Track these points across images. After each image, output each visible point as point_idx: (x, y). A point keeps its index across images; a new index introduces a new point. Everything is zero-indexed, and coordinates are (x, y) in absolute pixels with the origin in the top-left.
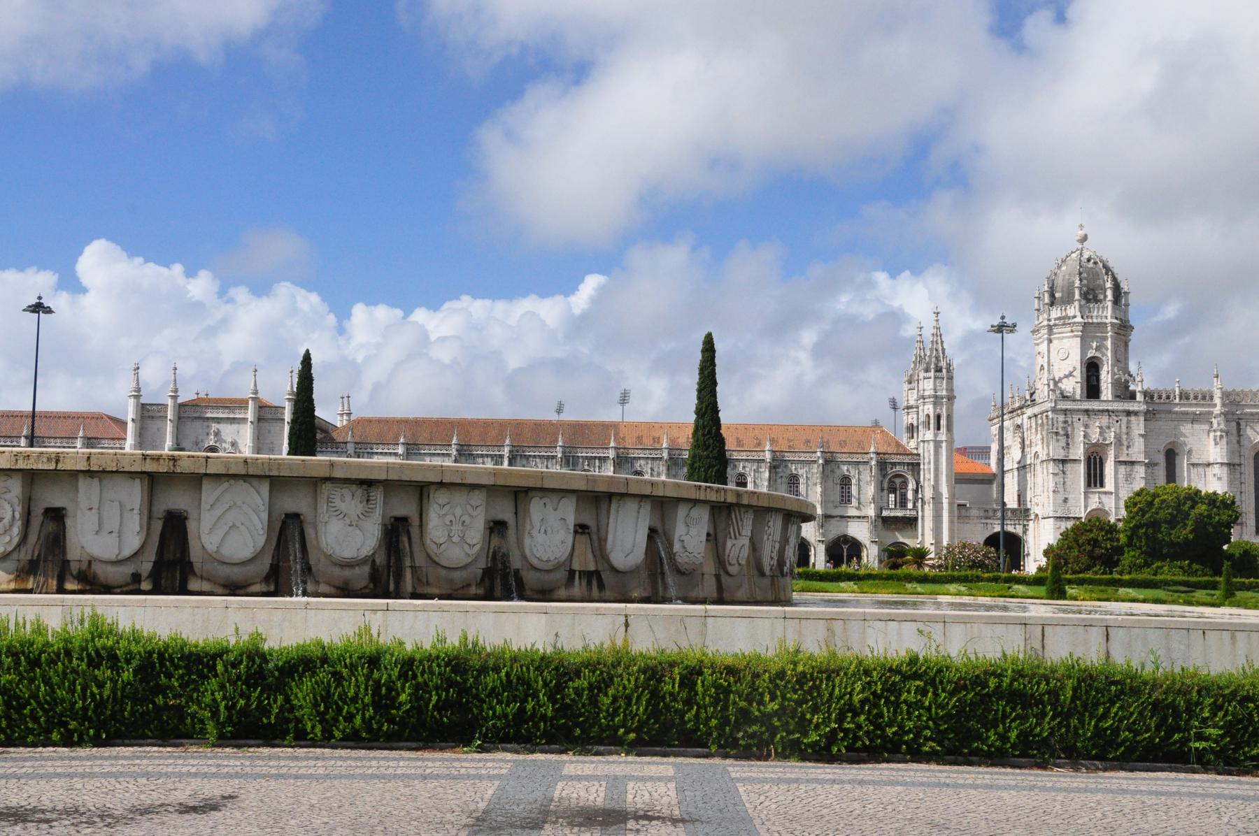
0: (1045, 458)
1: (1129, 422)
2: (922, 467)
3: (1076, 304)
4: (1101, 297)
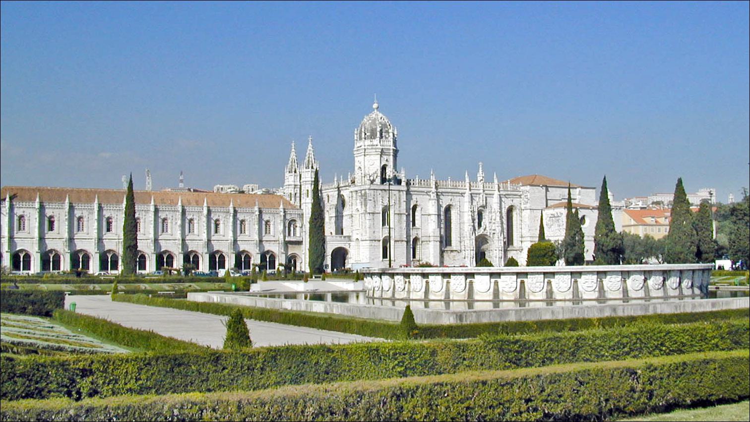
0: (363, 212)
1: (400, 195)
2: (304, 215)
3: (378, 139)
4: (387, 136)
